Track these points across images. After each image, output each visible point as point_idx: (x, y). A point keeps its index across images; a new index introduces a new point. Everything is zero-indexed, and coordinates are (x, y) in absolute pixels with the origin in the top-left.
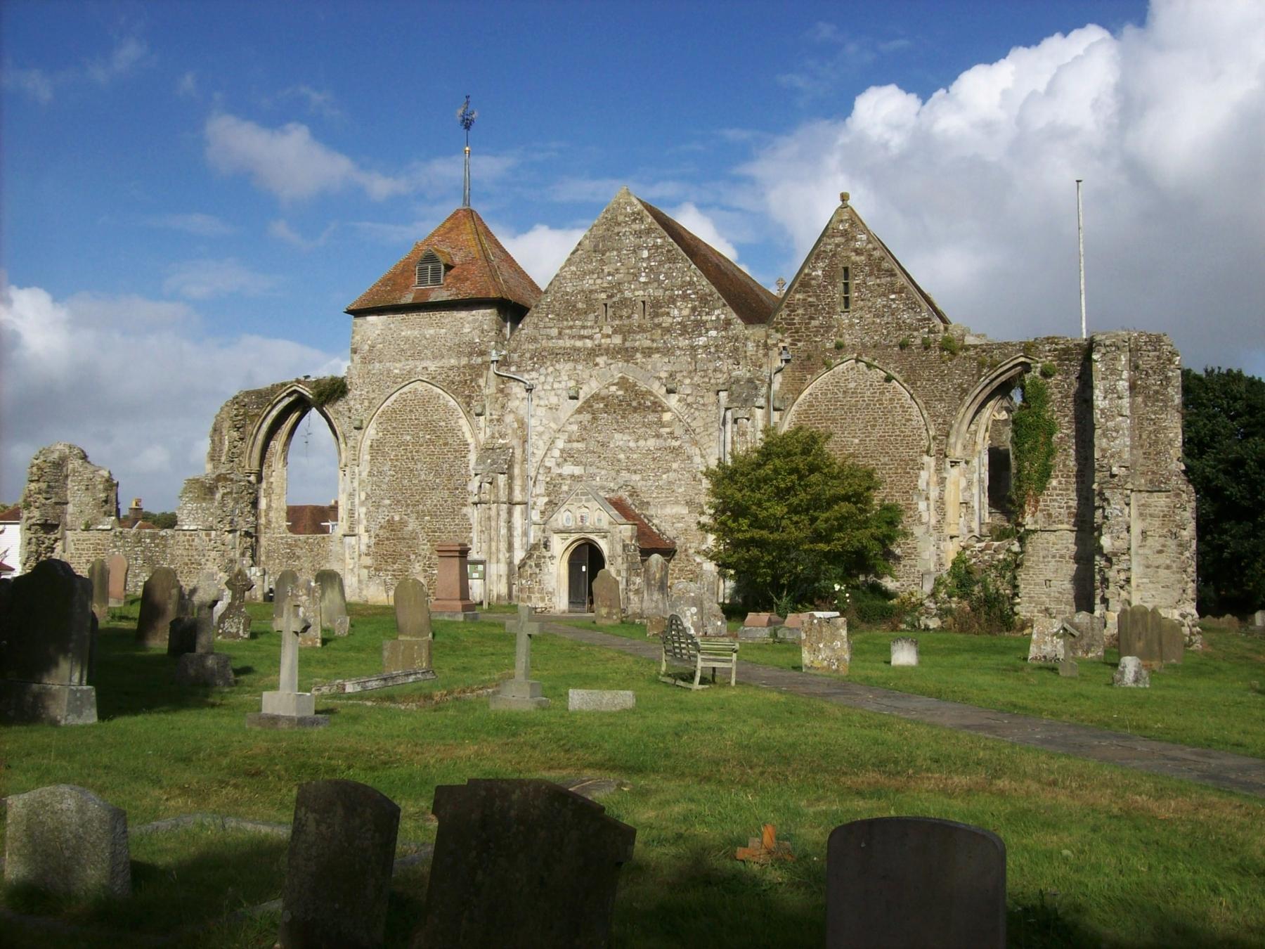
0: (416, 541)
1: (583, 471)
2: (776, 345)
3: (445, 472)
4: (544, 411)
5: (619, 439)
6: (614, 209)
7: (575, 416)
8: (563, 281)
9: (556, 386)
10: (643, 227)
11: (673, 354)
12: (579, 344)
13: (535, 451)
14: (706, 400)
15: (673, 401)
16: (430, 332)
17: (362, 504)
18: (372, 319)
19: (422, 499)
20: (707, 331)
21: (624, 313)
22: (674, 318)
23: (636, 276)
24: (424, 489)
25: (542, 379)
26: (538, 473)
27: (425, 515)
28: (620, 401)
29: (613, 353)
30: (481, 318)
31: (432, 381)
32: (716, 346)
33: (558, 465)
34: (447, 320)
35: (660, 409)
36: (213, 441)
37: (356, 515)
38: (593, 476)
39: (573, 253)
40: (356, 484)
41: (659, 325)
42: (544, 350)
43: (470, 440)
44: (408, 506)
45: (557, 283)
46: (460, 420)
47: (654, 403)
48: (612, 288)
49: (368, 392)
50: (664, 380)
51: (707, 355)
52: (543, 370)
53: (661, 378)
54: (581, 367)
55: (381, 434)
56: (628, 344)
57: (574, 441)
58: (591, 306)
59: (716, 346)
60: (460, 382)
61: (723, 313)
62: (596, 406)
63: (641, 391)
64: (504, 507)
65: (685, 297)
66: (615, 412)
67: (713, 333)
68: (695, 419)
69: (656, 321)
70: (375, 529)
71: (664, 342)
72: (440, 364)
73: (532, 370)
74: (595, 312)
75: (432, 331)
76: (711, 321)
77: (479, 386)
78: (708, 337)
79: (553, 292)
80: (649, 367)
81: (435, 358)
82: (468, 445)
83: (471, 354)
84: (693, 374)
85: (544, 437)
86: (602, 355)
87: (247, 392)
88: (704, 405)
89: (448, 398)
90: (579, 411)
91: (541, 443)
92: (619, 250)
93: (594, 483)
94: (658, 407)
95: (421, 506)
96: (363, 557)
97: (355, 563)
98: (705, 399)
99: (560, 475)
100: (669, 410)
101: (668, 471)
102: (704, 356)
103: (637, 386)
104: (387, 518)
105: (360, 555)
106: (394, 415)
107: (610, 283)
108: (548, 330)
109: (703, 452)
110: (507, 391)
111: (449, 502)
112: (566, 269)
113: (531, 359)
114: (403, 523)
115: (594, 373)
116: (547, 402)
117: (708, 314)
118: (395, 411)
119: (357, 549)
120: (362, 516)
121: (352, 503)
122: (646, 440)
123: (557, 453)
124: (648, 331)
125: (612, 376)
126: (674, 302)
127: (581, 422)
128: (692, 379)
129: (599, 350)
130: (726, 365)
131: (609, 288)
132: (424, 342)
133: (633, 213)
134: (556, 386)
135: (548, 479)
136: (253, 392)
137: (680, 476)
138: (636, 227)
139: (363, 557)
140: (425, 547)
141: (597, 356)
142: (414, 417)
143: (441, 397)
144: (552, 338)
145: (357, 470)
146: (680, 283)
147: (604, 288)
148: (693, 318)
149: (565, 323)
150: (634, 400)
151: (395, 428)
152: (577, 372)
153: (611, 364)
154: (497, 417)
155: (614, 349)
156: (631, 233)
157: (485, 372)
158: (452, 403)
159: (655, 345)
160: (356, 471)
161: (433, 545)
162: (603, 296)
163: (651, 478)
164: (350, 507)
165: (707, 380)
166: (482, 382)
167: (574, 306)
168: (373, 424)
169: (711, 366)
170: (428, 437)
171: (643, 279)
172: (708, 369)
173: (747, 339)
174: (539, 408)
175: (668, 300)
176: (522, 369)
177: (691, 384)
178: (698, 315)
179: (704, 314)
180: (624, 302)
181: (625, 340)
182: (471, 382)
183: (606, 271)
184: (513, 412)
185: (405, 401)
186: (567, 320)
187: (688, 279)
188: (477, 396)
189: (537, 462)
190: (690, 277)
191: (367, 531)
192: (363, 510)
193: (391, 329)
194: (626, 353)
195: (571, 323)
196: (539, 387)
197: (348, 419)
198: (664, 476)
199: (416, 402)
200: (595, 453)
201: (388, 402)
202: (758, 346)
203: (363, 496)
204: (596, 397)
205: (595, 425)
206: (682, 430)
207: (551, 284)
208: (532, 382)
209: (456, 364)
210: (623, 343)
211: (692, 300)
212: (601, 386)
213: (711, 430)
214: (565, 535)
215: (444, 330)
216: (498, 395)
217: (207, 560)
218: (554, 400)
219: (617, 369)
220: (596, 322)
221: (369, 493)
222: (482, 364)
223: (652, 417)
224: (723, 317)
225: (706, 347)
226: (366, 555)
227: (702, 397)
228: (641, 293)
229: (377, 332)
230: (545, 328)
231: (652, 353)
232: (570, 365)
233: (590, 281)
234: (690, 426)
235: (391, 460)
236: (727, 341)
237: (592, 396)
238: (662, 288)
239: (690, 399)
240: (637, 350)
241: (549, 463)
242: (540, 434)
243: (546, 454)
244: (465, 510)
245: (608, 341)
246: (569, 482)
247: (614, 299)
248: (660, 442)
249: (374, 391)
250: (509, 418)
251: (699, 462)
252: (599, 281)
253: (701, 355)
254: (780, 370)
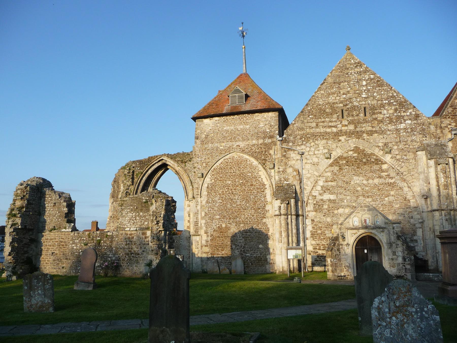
0: (236, 238)
1: (336, 197)
2: (446, 127)
3: (252, 200)
4: (310, 166)
5: (357, 180)
6: (344, 62)
7: (329, 168)
8: (317, 99)
9: (316, 152)
10: (362, 70)
11: (385, 134)
12: (329, 130)
13: (306, 187)
14: (408, 157)
15: (388, 158)
17: (202, 218)
18: (206, 121)
19: (239, 215)
20: (405, 121)
21: (354, 113)
22: (384, 115)
23: (360, 94)
24: (240, 209)
25: (308, 149)
26: (308, 199)
27: (240, 224)
28: (356, 159)
29: (349, 134)
30: (269, 119)
31: (243, 151)
32: (411, 128)
33: (320, 194)
34: (250, 121)
35: (380, 162)
36: (114, 187)
37: (199, 225)
38: (342, 200)
39: (322, 84)
40: (199, 207)
41: (376, 119)
42: (308, 134)
43: (267, 183)
44: (230, 218)
45: (314, 100)
46: (259, 172)
47: (376, 160)
48: (347, 100)
49: (205, 159)
50: (381, 148)
51: (406, 133)
52: (308, 145)
53: (379, 146)
54: (331, 142)
55: (213, 180)
56: (358, 129)
57: (329, 181)
58: (334, 111)
59: (411, 128)
60: (259, 152)
61: (414, 111)
62: (341, 162)
63: (368, 154)
64: (294, 217)
65: (390, 104)
66: (353, 165)
67: (409, 122)
68: (402, 167)
69: (374, 116)
70: (210, 231)
71: (380, 127)
72: (247, 143)
73: (302, 145)
74: (337, 114)
75: (242, 127)
76: (407, 115)
77: (270, 154)
78: (406, 124)
79: (311, 104)
80: (372, 141)
81: (244, 140)
82: (265, 185)
83: (264, 138)
84: (399, 144)
85: (311, 180)
86: (343, 135)
87: (134, 162)
88: (407, 160)
89: (252, 160)
90: (331, 165)
91: (309, 183)
92: (348, 82)
93: (343, 204)
94: (378, 161)
95: (238, 219)
96: (204, 247)
97: (199, 251)
98: (407, 156)
99: (322, 200)
100: (386, 163)
101: (388, 196)
102: (404, 134)
103: (365, 151)
104: (218, 226)
105: (202, 246)
106: (221, 171)
107: (344, 98)
108: (310, 124)
109: (409, 185)
110: (287, 156)
111: (255, 216)
112: (318, 92)
113: (300, 139)
114: (227, 228)
115: (339, 145)
116: (311, 161)
117: (404, 112)
118: (221, 169)
119: (200, 242)
120: (203, 225)
121: (196, 218)
122: (373, 179)
123: (319, 188)
124: (370, 122)
125: (350, 146)
126: (384, 107)
127: (333, 171)
128: (398, 146)
129: (341, 133)
130: (418, 138)
131: (344, 101)
132: (237, 132)
133: (355, 63)
134: (316, 152)
135: (315, 202)
136: (138, 161)
137: (396, 198)
138: (358, 70)
139: (204, 247)
140: (241, 241)
141: (340, 136)
142: (232, 171)
143: (248, 161)
144: (313, 128)
145: (199, 200)
146: (386, 97)
147: (341, 101)
148: (395, 114)
149: (320, 120)
150: (364, 158)
151: (221, 177)
152: (329, 145)
153: (349, 140)
154: (282, 170)
155: (350, 132)
156: (355, 73)
157: (274, 147)
158: (255, 162)
159: (374, 129)
160: (199, 201)
161: (246, 240)
162: (341, 105)
163: (378, 200)
164: (195, 220)
165: (408, 147)
166: (272, 152)
167: (324, 111)
168: (209, 176)
169: (410, 139)
170: (241, 181)
171: (364, 96)
172: (407, 141)
173: (430, 124)
174: (306, 164)
175: (380, 106)
176: (296, 144)
177: (398, 149)
178: (399, 113)
179: (402, 112)
181: (356, 127)
182: (265, 152)
183: (342, 92)
184: (292, 167)
185: (226, 163)
186: (321, 118)
187: (391, 95)
188: (269, 159)
189: (307, 193)
190: (392, 93)
191: (206, 233)
192: (204, 221)
193: (217, 126)
194: (358, 135)
195: (323, 120)
196: (306, 153)
197: (194, 173)
198: (386, 199)
199: (233, 163)
200: (342, 187)
201: (217, 164)
202: (436, 127)
203: (203, 214)
204: (341, 158)
205: (341, 172)
206: (395, 174)
207: (310, 100)
208: (302, 151)
209: (257, 143)
210: (355, 129)
211: (395, 105)
212: (343, 152)
213: (412, 173)
214: (355, 231)
215: (248, 126)
216: (282, 158)
217: (143, 251)
218: (316, 160)
219: (353, 143)
220: (338, 119)
221: (207, 212)
222: (271, 143)
223: (376, 167)
224: (414, 113)
225: (405, 129)
226: (205, 246)
227: (406, 155)
228: (364, 103)
229: (210, 128)
230: (308, 122)
231: (373, 133)
232: (324, 141)
233: (332, 98)
234: (400, 172)
235: (219, 194)
236: (418, 125)
237: (339, 157)
238: (376, 100)
239: (398, 157)
240: (364, 132)
241: (315, 193)
242: (308, 178)
243: (312, 188)
244: (264, 220)
245: (346, 128)
246: (327, 203)
247: (348, 107)
248: (382, 181)
249: (209, 158)
250: (290, 170)
251: (407, 190)
252: (338, 98)
253: (403, 134)
254: (451, 140)
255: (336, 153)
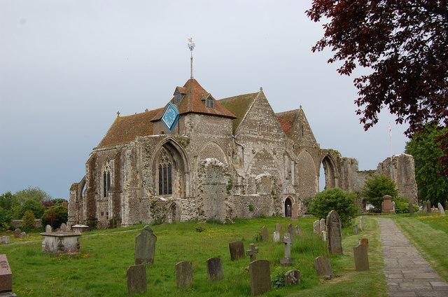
5: (264, 167)
16: (215, 125)
18: (197, 116)
29: (263, 141)
90: (255, 157)
94: (271, 158)
180: (263, 126)
194: (264, 141)
219: (263, 146)
250: (238, 158)
255: (257, 151)
